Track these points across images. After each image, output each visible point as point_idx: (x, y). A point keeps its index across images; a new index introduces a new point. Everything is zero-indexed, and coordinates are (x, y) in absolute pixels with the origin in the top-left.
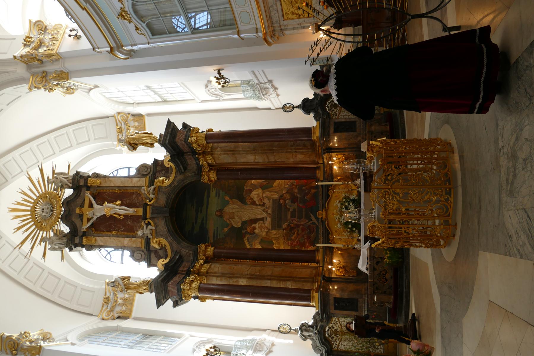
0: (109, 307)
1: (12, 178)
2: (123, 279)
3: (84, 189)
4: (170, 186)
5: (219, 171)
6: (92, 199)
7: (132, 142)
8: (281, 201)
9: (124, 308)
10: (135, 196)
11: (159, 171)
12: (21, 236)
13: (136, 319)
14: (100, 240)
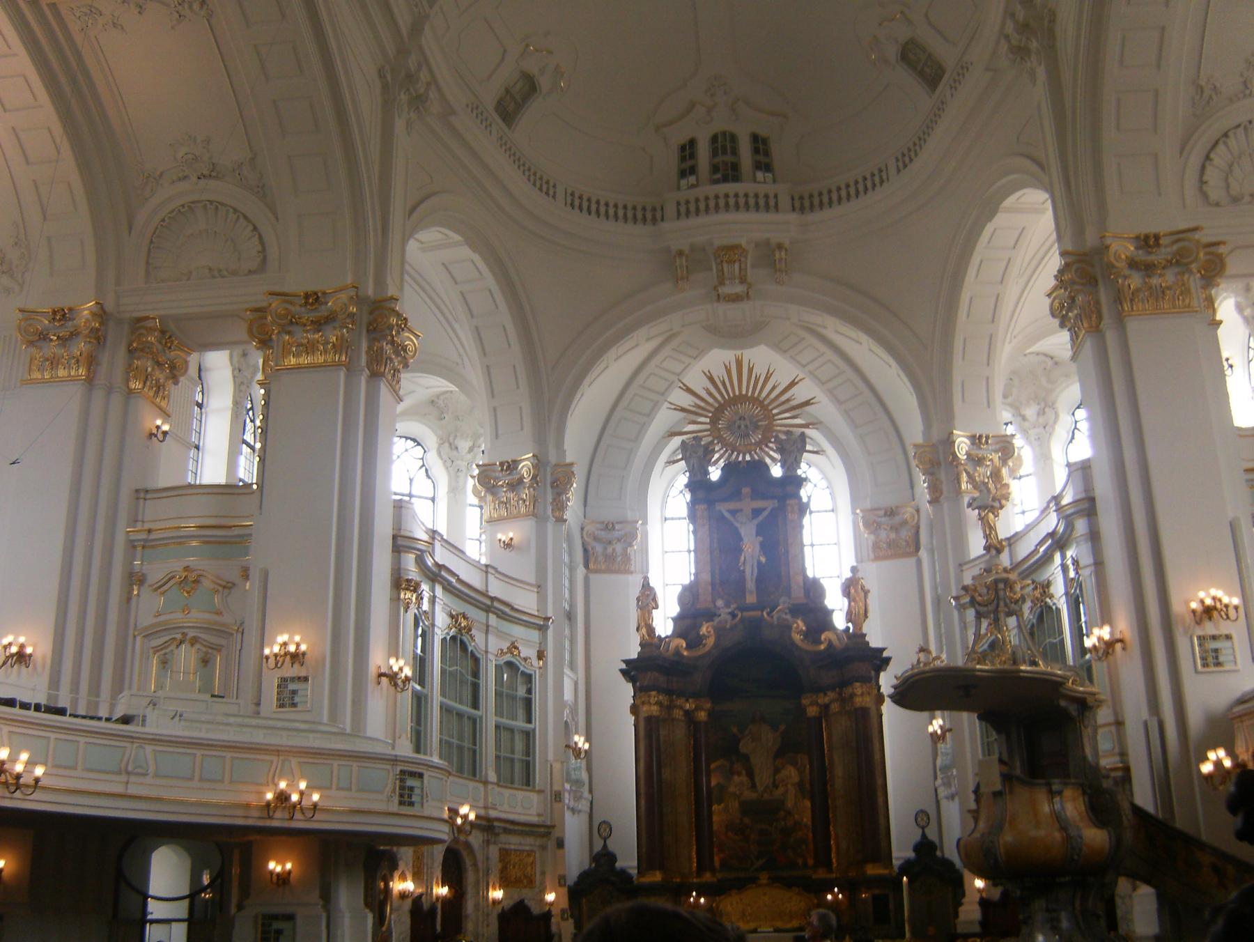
0: (599, 532)
1: (791, 357)
2: (654, 599)
4: (793, 644)
5: (818, 720)
7: (852, 591)
8: (782, 813)
9: (600, 559)
13: (587, 580)
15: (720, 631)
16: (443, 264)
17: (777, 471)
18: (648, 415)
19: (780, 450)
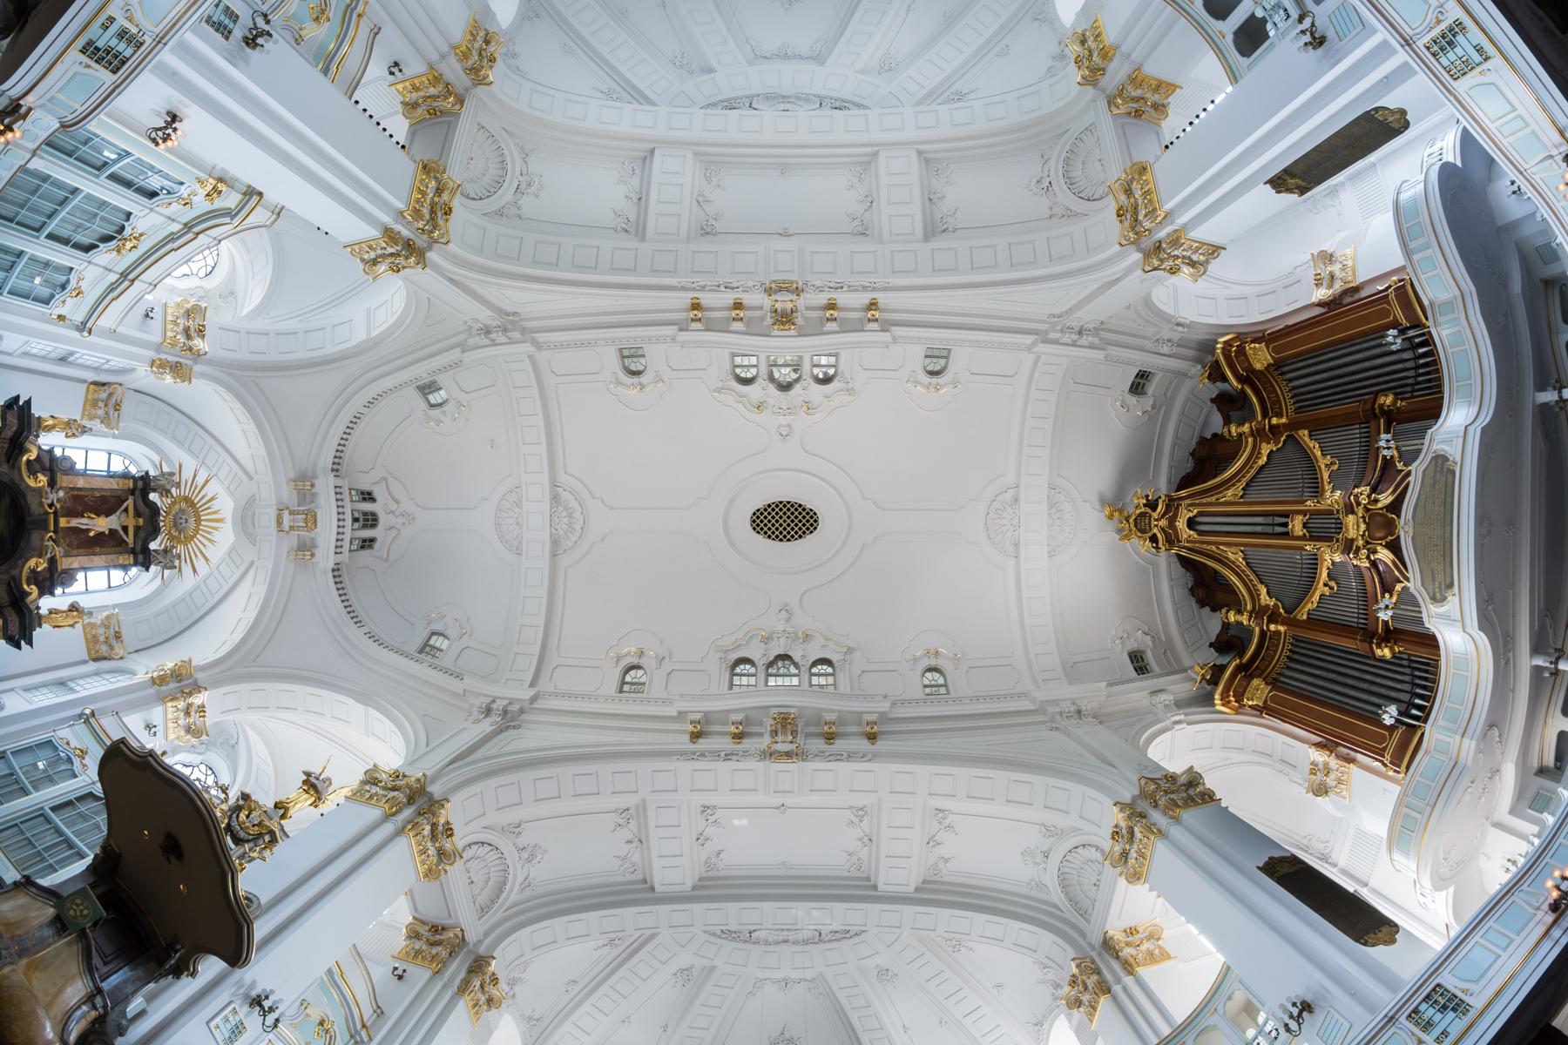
3: (138, 549)
6: (125, 538)
10: (75, 543)
11: (45, 580)
12: (210, 490)
14: (113, 484)
15: (39, 491)
16: (351, 320)
17: (153, 546)
18: (189, 449)
19: (166, 551)
